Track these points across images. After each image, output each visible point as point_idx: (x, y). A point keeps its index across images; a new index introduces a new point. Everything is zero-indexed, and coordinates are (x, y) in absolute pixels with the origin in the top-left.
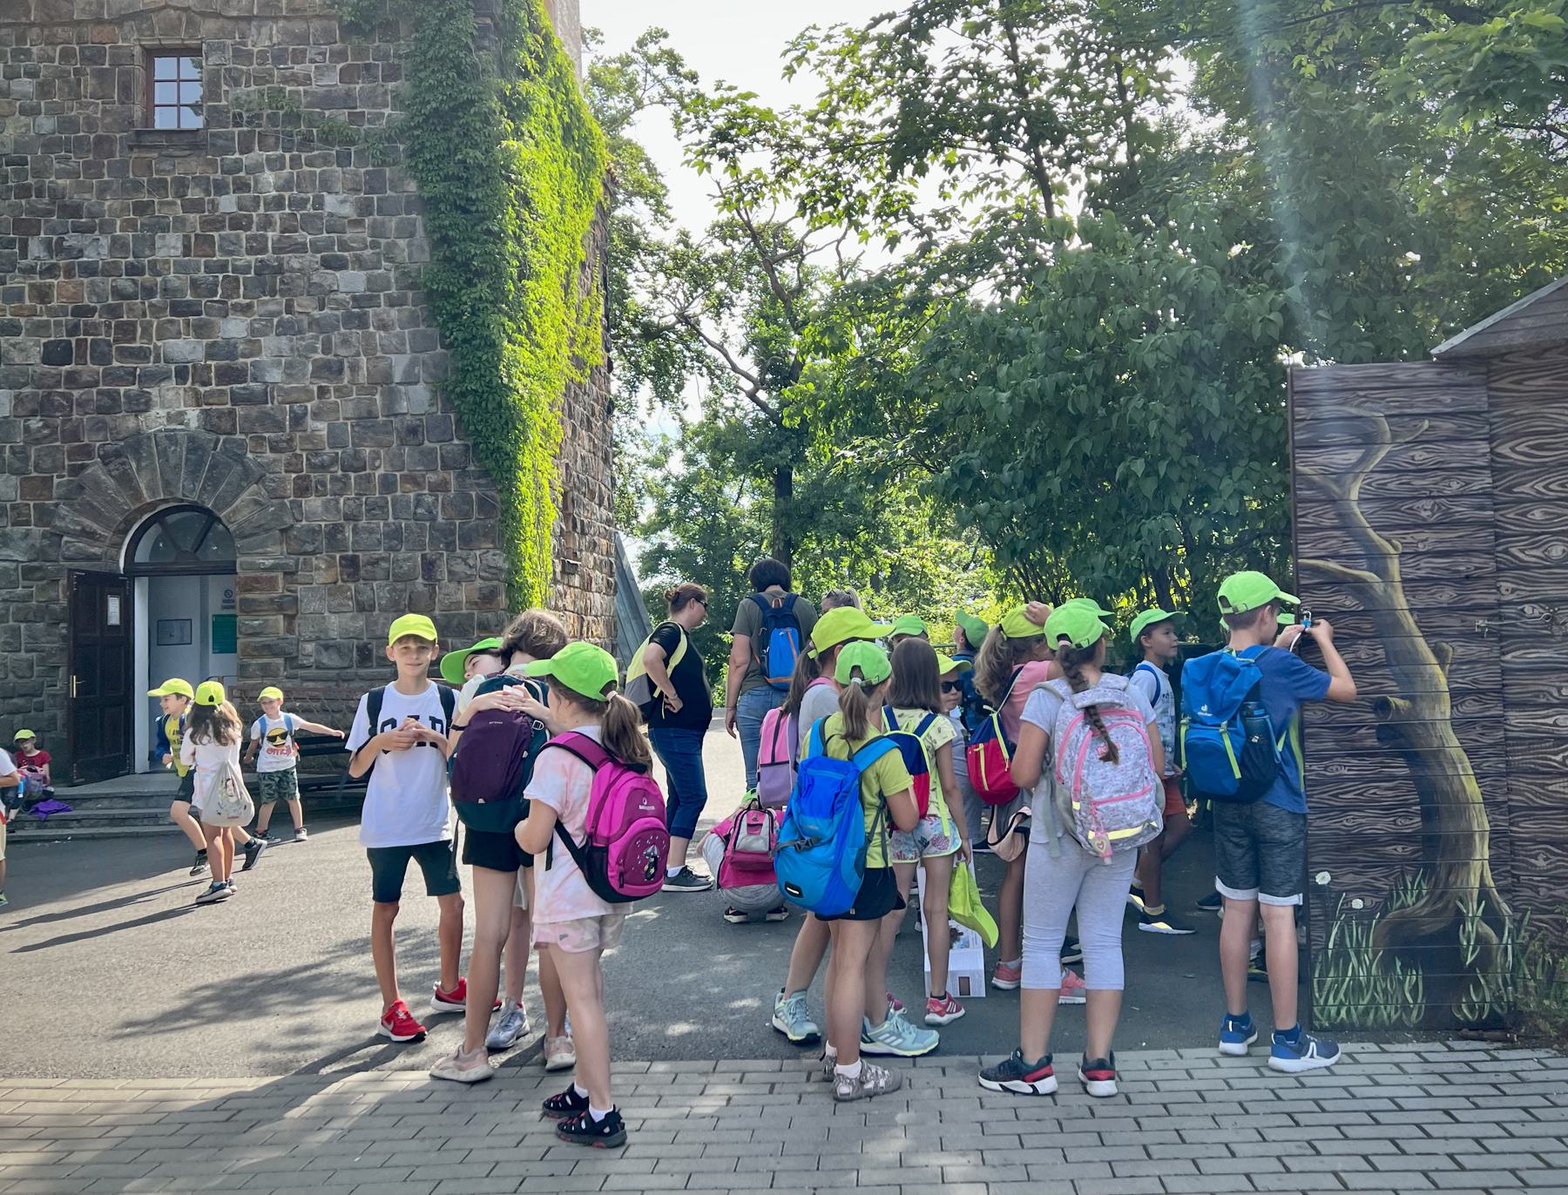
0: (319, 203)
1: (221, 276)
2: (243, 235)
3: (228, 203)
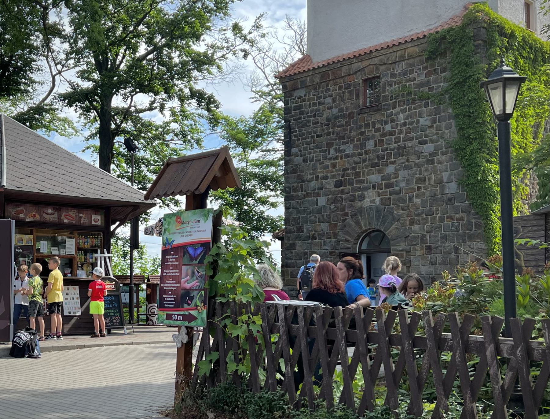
3: (388, 127)
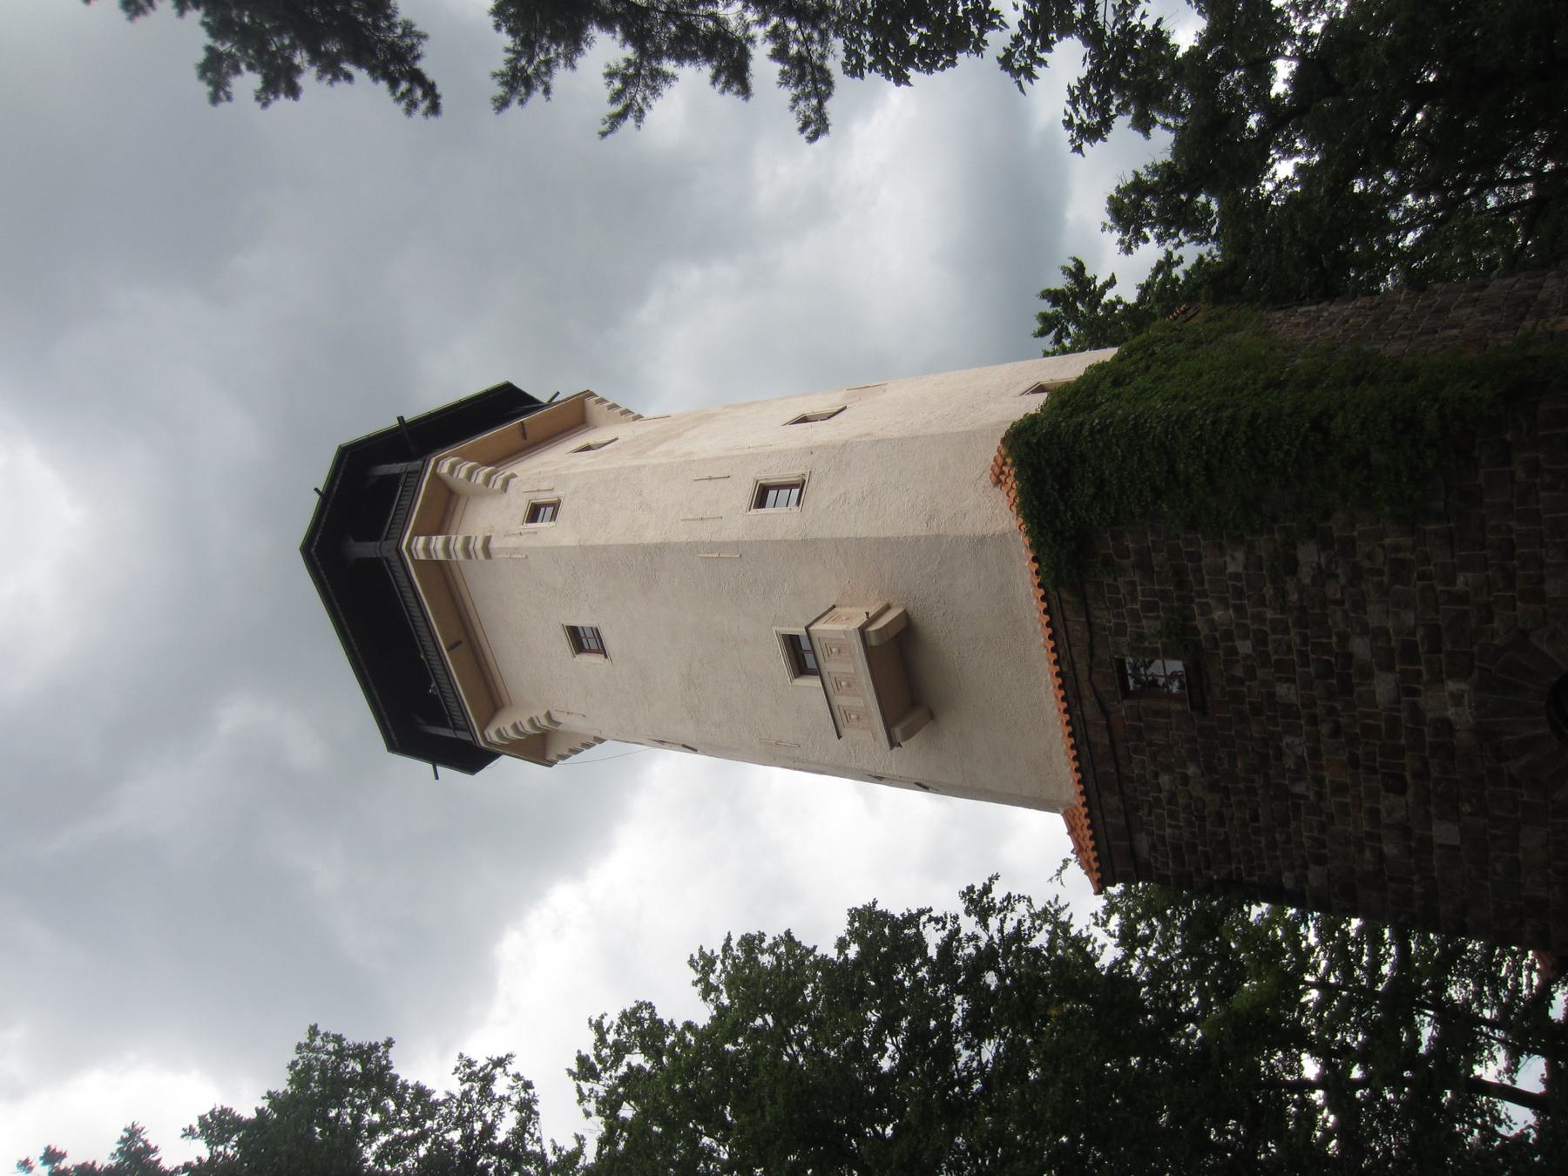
0: (1237, 576)
1: (1312, 656)
2: (1272, 637)
3: (1245, 647)
